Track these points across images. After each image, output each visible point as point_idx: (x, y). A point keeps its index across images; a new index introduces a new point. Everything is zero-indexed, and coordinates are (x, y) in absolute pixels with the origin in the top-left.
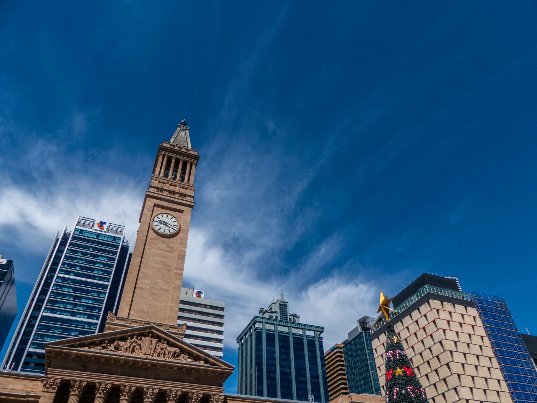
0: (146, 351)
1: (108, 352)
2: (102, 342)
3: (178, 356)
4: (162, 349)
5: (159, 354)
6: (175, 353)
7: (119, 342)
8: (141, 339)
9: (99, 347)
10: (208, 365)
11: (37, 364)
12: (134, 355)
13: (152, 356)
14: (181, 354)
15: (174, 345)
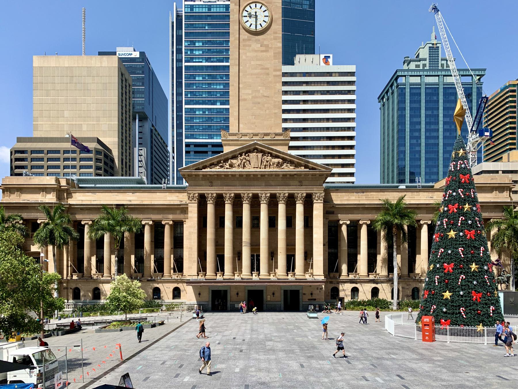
0: (254, 164)
1: (226, 170)
2: (219, 162)
3: (282, 165)
4: (267, 162)
5: (266, 165)
6: (279, 163)
7: (232, 161)
8: (248, 156)
9: (218, 167)
10: (308, 170)
11: (196, 152)
12: (246, 170)
13: (260, 168)
14: (284, 163)
15: (277, 157)
